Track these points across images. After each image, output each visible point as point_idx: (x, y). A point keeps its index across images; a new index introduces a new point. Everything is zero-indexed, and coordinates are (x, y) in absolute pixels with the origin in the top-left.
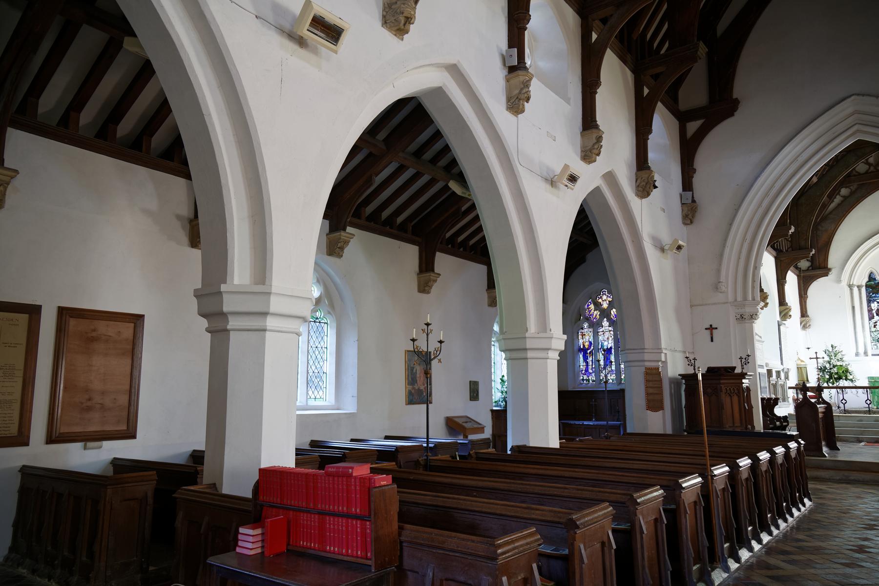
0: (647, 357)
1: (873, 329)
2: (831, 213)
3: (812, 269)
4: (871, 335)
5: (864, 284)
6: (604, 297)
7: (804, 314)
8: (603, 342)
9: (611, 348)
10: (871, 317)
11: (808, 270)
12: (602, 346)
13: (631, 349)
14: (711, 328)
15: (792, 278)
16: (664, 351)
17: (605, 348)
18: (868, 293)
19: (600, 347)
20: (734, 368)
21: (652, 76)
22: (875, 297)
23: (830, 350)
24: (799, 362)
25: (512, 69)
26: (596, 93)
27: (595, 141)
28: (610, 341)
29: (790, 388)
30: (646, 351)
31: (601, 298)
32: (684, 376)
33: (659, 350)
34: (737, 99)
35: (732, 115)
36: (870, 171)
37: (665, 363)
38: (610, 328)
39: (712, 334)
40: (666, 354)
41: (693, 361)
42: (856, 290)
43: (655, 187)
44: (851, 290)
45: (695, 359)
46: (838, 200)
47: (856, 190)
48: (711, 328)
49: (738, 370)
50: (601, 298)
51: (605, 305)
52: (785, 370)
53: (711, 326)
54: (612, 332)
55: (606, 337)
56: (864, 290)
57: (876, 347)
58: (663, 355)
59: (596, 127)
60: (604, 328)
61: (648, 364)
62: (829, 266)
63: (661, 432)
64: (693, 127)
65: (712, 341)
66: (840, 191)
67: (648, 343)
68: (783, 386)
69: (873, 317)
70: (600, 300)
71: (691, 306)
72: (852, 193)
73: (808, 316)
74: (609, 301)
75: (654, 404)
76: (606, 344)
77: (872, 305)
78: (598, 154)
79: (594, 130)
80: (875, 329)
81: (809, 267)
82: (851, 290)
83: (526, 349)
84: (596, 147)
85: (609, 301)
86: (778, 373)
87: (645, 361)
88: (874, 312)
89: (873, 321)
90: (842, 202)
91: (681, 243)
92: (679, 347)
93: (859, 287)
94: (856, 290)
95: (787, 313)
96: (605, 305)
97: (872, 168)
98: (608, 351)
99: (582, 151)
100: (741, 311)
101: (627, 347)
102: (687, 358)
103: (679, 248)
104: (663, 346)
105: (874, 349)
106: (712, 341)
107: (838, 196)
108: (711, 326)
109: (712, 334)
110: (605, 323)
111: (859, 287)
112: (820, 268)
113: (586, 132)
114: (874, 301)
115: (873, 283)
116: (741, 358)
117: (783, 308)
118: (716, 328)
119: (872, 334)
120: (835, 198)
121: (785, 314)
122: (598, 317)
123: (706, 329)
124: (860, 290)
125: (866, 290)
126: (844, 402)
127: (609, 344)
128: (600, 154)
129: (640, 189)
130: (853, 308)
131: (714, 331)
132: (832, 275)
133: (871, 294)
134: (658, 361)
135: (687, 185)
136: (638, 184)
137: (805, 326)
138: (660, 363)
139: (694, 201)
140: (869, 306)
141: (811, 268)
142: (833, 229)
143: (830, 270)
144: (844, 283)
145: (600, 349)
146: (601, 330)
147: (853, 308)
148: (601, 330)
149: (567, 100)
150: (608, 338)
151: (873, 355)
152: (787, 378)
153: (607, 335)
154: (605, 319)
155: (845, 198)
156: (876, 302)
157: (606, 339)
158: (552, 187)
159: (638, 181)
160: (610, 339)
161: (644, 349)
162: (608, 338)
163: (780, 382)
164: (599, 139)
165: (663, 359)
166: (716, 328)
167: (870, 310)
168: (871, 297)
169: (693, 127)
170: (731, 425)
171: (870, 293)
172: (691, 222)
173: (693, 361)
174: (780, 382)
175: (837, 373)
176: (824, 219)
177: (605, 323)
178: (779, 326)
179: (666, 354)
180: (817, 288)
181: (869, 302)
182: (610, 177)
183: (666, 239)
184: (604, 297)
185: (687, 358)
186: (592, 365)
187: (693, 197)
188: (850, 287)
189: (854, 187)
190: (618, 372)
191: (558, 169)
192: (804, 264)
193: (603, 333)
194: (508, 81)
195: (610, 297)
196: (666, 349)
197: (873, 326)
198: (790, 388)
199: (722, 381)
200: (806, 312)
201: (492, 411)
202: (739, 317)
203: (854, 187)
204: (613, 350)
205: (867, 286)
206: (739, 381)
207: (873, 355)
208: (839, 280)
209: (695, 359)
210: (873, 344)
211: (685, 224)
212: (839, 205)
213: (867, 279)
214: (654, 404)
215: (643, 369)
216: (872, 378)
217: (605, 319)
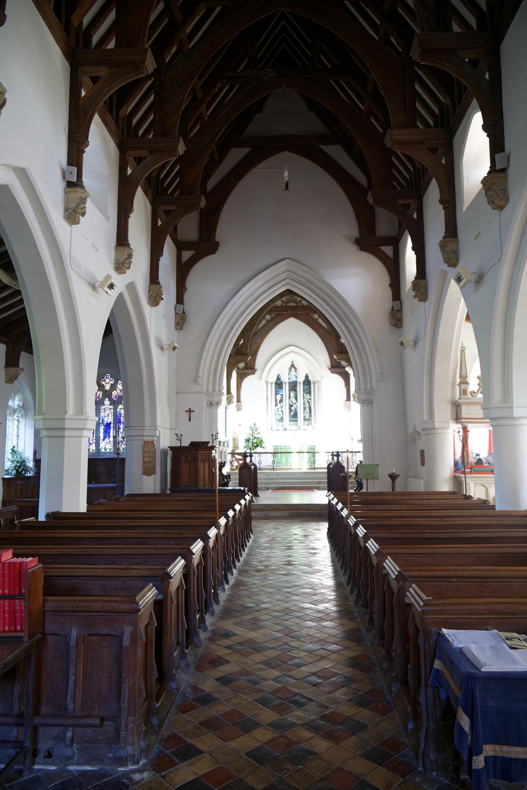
0: (146, 433)
1: (277, 413)
2: (259, 330)
3: (246, 369)
5: (274, 382)
6: (107, 380)
7: (238, 401)
8: (104, 417)
9: (110, 423)
10: (276, 405)
11: (243, 369)
12: (103, 421)
13: (134, 426)
14: (190, 411)
15: (234, 374)
16: (159, 429)
17: (105, 422)
18: (276, 388)
19: (101, 422)
20: (208, 443)
21: (165, 211)
22: (279, 391)
23: (253, 426)
24: (234, 435)
25: (70, 184)
26: (129, 217)
27: (126, 257)
28: (110, 418)
29: (229, 453)
30: (145, 428)
31: (104, 381)
32: (171, 448)
33: (154, 426)
34: (218, 242)
35: (214, 253)
36: (283, 306)
37: (159, 437)
38: (111, 407)
39: (190, 415)
40: (159, 431)
41: (180, 437)
42: (269, 385)
43: (162, 299)
44: (267, 385)
45: (181, 435)
46: (264, 322)
47: (274, 317)
48: (190, 411)
49: (210, 445)
50: (104, 381)
51: (108, 387)
52: (227, 441)
53: (190, 409)
54: (112, 410)
55: (107, 413)
56: (274, 385)
58: (158, 431)
59: (128, 245)
60: (105, 406)
61: (146, 439)
62: (256, 368)
63: (153, 492)
64: (187, 255)
65: (190, 420)
66: (265, 316)
67: (148, 422)
68: (225, 452)
70: (104, 383)
71: (177, 393)
72: (272, 319)
73: (241, 402)
74: (111, 384)
75: (148, 471)
76: (106, 419)
78: (129, 268)
79: (126, 248)
81: (244, 367)
82: (267, 385)
83: (64, 429)
84: (127, 262)
85: (111, 384)
86: (224, 443)
87: (144, 436)
89: (277, 407)
90: (266, 324)
91: (176, 345)
92: (168, 425)
93: (271, 383)
94: (269, 385)
95: (231, 400)
96: (108, 387)
97: (284, 304)
98: (108, 426)
99: (115, 263)
100: (210, 399)
101: (131, 425)
102: (176, 434)
103: (174, 348)
104: (158, 424)
106: (190, 420)
107: (264, 320)
108: (190, 409)
109: (190, 415)
110: (107, 402)
111: (271, 383)
112: (250, 368)
113: (119, 248)
114: (279, 393)
115: (279, 381)
116: (212, 435)
117: (229, 396)
118: (193, 411)
120: (262, 320)
121: (229, 401)
122: (101, 396)
123: (186, 411)
124: (271, 386)
125: (275, 386)
126: (260, 462)
127: (110, 419)
128: (129, 268)
129: (151, 299)
130: (267, 397)
131: (192, 413)
132: (257, 374)
134: (154, 436)
135: (180, 300)
136: (150, 295)
137: (239, 409)
138: (155, 438)
139: (184, 313)
140: (276, 397)
141: (245, 368)
142: (259, 342)
143: (256, 370)
144: (263, 381)
145: (101, 424)
146: (103, 408)
147: (267, 397)
148: (103, 408)
149: (107, 218)
150: (108, 415)
151: (276, 430)
152: (228, 446)
153: (108, 412)
154: (107, 399)
155: (268, 321)
156: (279, 395)
157: (106, 415)
158: (93, 290)
159: (151, 292)
160: (110, 415)
161: (144, 426)
162: (108, 415)
163: (224, 450)
164: (130, 256)
165: (158, 435)
166: (193, 411)
167: (276, 400)
168: (277, 391)
169: (187, 255)
170: (203, 484)
172: (181, 329)
173: (180, 437)
174: (224, 450)
175: (256, 443)
176: (255, 334)
177: (107, 402)
178: (226, 408)
179: (159, 431)
180: (248, 381)
181: (276, 394)
182: (131, 287)
183: (165, 341)
184: (107, 380)
185: (176, 434)
186: (93, 437)
187: (183, 309)
188: (267, 383)
189: (273, 315)
190: (116, 443)
191: (101, 277)
192: (242, 365)
193: (104, 410)
194: (66, 193)
195: (112, 381)
196: (160, 427)
198: (229, 453)
199: (199, 452)
200: (240, 399)
201: (4, 479)
202: (209, 403)
203: (273, 315)
204: (112, 425)
205: (276, 384)
206: (210, 452)
207: (276, 430)
208: (261, 378)
209: (181, 435)
211: (177, 329)
212: (264, 326)
213: (276, 379)
214: (148, 471)
215: (142, 443)
216: (275, 446)
217: (107, 399)
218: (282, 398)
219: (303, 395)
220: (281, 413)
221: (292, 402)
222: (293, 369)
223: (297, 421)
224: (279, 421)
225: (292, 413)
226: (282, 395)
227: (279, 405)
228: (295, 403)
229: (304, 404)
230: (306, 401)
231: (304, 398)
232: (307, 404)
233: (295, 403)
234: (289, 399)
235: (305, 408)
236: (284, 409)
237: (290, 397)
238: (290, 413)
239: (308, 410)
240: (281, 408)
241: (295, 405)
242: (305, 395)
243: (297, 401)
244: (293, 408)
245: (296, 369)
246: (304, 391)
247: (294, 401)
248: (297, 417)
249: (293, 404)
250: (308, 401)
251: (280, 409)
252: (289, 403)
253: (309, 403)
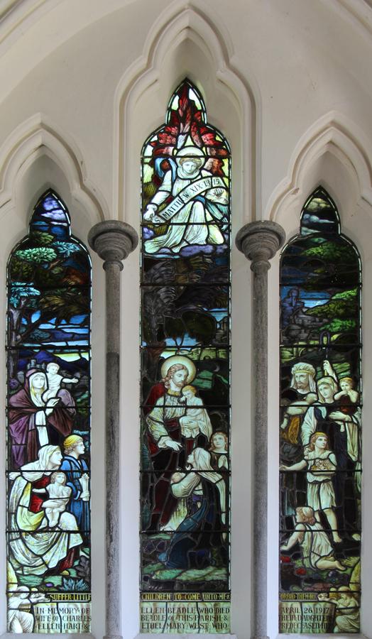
1: (26, 520)
4: (11, 554)
10: (22, 453)
22: (53, 335)
57: (28, 617)
69: (31, 453)
77: (36, 381)
80: (35, 518)
88: (40, 418)
89: (33, 470)
105: (18, 628)
119: (18, 546)
133: (35, 318)
167: (20, 411)
171: (27, 313)
197: (26, 500)
210: (15, 602)
218: (79, 390)
219: (286, 371)
220: (69, 522)
221: (173, 428)
222: (189, 148)
223: (221, 588)
224: (47, 591)
225: (173, 524)
226: (82, 366)
227: (49, 456)
228: (203, 441)
229: (292, 449)
230: (310, 423)
231: (289, 395)
232: (318, 450)
233: (203, 441)
234: (147, 406)
235: (294, 487)
236: (92, 488)
237: (152, 389)
238: (149, 526)
239: (323, 499)
240: (71, 479)
241: (200, 458)
242: (301, 371)
243: (221, 422)
244: (181, 484)
245: (220, 150)
246: (288, 339)
247: (196, 421)
248: (224, 561)
249: (188, 446)
250: (326, 426)
251: (58, 489)
252: (148, 440)
253: (336, 441)
